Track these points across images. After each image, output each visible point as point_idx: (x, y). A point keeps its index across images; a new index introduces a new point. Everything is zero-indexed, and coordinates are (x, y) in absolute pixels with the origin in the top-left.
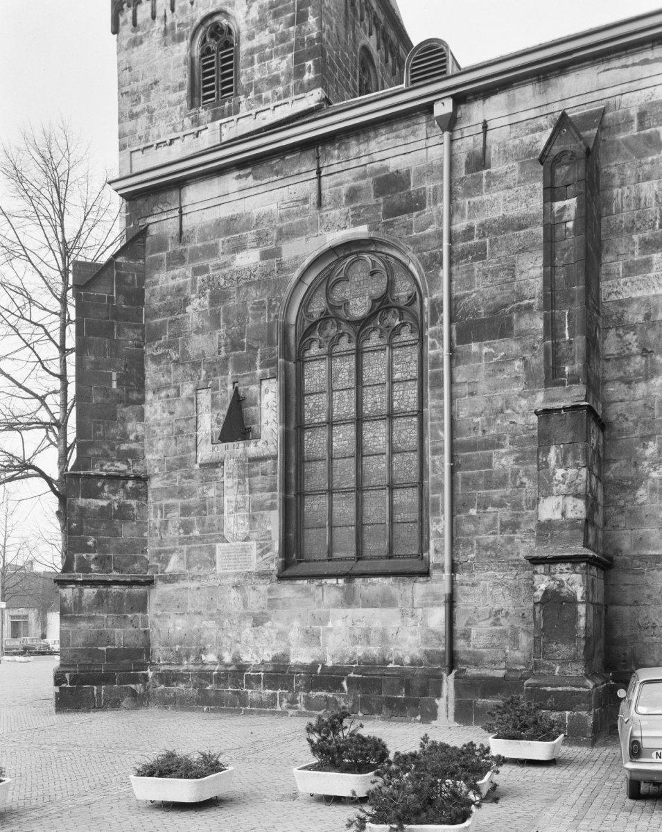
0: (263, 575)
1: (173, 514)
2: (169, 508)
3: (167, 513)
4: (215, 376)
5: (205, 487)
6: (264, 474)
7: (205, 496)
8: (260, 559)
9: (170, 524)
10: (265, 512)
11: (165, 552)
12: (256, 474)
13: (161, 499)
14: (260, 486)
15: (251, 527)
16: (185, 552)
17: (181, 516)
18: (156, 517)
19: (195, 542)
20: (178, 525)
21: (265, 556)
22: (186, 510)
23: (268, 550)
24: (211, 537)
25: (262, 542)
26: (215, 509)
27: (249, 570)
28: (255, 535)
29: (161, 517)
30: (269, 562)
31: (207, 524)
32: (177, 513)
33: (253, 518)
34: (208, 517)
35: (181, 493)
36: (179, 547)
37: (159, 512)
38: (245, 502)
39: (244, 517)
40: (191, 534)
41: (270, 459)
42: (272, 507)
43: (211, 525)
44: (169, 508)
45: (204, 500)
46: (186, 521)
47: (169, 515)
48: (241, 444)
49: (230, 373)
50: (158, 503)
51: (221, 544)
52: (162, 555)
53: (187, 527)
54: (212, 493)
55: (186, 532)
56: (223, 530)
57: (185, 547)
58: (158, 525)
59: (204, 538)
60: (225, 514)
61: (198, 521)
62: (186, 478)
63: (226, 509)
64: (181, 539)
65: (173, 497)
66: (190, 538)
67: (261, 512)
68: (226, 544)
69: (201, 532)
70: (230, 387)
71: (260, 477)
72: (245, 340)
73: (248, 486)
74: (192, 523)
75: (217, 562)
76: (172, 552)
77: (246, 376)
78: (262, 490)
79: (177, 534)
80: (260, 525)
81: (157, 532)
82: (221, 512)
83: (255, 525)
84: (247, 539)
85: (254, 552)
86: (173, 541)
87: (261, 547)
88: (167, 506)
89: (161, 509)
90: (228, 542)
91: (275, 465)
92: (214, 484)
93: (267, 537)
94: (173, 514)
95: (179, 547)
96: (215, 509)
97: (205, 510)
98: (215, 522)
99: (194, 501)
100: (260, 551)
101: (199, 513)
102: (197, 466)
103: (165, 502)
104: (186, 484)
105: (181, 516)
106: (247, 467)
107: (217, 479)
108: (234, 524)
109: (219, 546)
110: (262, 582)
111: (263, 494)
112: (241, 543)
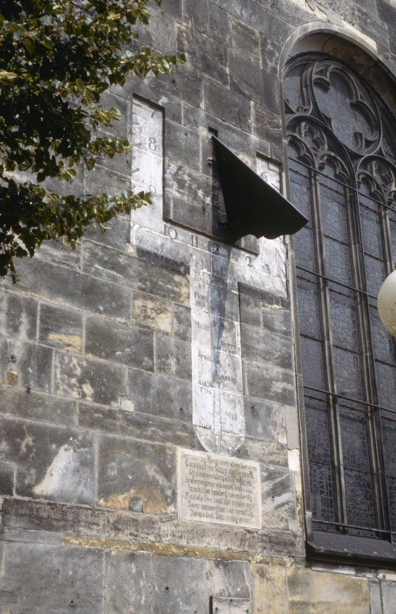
0: (276, 542)
1: (66, 339)
2: (52, 320)
3: (46, 331)
4: (175, 93)
5: (150, 305)
6: (268, 326)
7: (149, 322)
8: (270, 505)
9: (55, 361)
10: (275, 405)
11: (38, 433)
12: (255, 322)
13: (34, 288)
14: (261, 346)
15: (249, 429)
16: (96, 447)
17: (89, 349)
18: (15, 329)
19: (123, 430)
20: (78, 371)
21: (279, 500)
22: (100, 340)
23: (282, 487)
24: (165, 427)
25: (272, 468)
26: (172, 362)
27: (250, 527)
28: (256, 447)
29: (31, 334)
30: (285, 515)
31: (152, 391)
32: (78, 340)
33: (252, 411)
34: (156, 377)
35: (90, 293)
36: (80, 430)
37: (24, 319)
38: (234, 369)
39: (233, 401)
40: (115, 405)
41: (277, 303)
42: (284, 398)
43: (163, 396)
44: (52, 320)
45: (146, 332)
46: (100, 367)
47: (53, 337)
48: (223, 251)
49: (202, 105)
50: (21, 294)
51: (188, 452)
52: (29, 440)
53: (106, 385)
54: (165, 323)
55: (100, 397)
56: (190, 417)
57: (96, 435)
58: (18, 352)
59: (146, 425)
60: (195, 381)
61: (134, 377)
62: (104, 264)
63: (195, 372)
64: (84, 411)
65: (70, 296)
66: (111, 414)
67: (267, 402)
68: (198, 454)
69: (139, 407)
70: (204, 133)
71: (262, 331)
72: (228, 70)
73: (238, 338)
74: (115, 378)
75: (179, 491)
76: (62, 439)
77: (234, 131)
78: (267, 356)
79: (75, 395)
80: (265, 429)
81: (14, 369)
82: (185, 373)
83: (256, 426)
84: (241, 453)
85: (259, 487)
86: (66, 409)
87: (270, 476)
88: (48, 311)
89: (32, 313)
90: (201, 448)
91: (287, 317)
92: (171, 307)
93: (280, 458)
94: (66, 339)
95: (80, 430)
96: (172, 362)
97: (151, 356)
98: (173, 392)
99: (122, 325)
100: (268, 486)
101: (134, 360)
102: (131, 250)
103: (43, 299)
104: (104, 276)
105: (89, 349)
106: (236, 299)
107: (176, 296)
108: (215, 408)
109: (182, 453)
110: (277, 557)
111: (270, 365)
112: (225, 457)
